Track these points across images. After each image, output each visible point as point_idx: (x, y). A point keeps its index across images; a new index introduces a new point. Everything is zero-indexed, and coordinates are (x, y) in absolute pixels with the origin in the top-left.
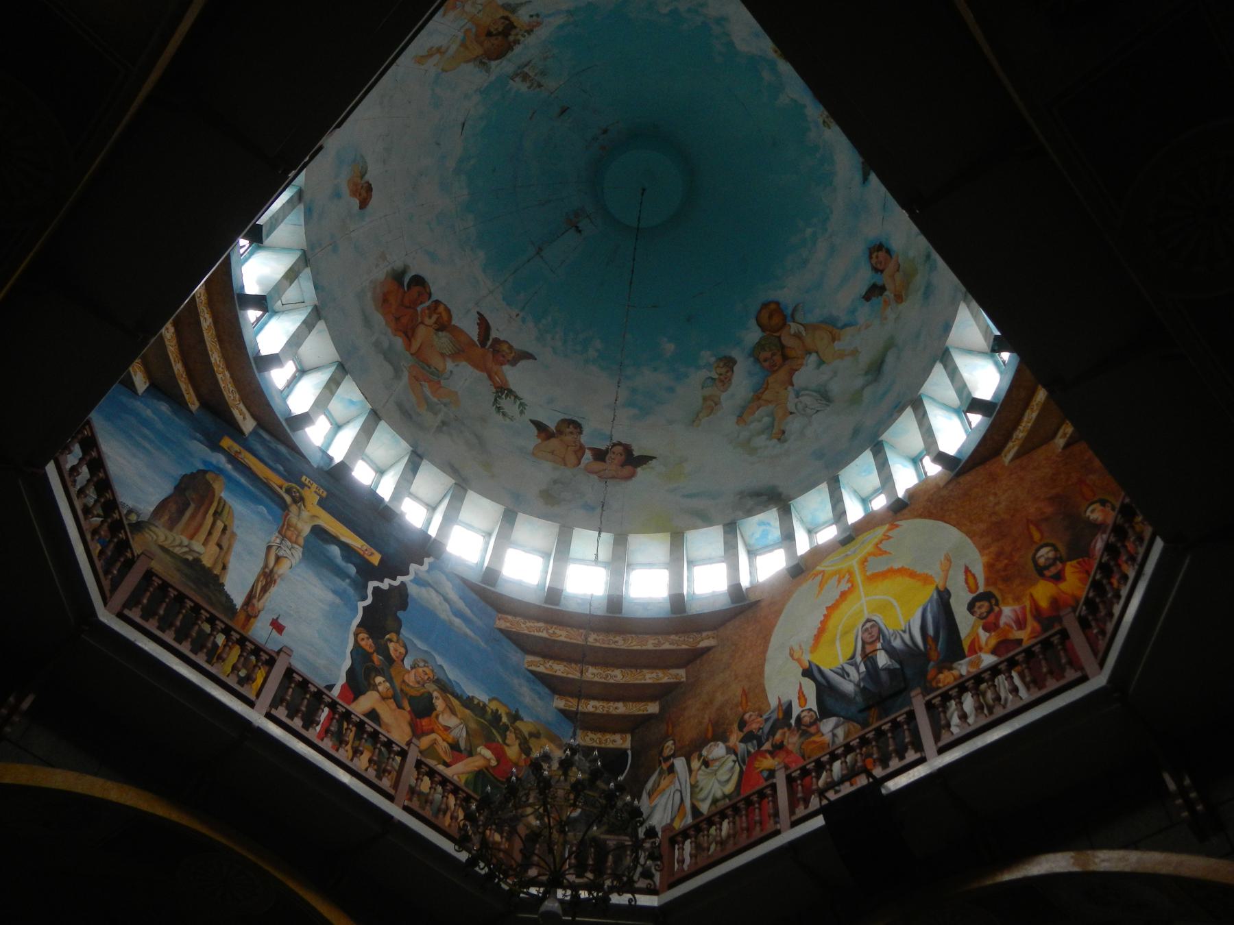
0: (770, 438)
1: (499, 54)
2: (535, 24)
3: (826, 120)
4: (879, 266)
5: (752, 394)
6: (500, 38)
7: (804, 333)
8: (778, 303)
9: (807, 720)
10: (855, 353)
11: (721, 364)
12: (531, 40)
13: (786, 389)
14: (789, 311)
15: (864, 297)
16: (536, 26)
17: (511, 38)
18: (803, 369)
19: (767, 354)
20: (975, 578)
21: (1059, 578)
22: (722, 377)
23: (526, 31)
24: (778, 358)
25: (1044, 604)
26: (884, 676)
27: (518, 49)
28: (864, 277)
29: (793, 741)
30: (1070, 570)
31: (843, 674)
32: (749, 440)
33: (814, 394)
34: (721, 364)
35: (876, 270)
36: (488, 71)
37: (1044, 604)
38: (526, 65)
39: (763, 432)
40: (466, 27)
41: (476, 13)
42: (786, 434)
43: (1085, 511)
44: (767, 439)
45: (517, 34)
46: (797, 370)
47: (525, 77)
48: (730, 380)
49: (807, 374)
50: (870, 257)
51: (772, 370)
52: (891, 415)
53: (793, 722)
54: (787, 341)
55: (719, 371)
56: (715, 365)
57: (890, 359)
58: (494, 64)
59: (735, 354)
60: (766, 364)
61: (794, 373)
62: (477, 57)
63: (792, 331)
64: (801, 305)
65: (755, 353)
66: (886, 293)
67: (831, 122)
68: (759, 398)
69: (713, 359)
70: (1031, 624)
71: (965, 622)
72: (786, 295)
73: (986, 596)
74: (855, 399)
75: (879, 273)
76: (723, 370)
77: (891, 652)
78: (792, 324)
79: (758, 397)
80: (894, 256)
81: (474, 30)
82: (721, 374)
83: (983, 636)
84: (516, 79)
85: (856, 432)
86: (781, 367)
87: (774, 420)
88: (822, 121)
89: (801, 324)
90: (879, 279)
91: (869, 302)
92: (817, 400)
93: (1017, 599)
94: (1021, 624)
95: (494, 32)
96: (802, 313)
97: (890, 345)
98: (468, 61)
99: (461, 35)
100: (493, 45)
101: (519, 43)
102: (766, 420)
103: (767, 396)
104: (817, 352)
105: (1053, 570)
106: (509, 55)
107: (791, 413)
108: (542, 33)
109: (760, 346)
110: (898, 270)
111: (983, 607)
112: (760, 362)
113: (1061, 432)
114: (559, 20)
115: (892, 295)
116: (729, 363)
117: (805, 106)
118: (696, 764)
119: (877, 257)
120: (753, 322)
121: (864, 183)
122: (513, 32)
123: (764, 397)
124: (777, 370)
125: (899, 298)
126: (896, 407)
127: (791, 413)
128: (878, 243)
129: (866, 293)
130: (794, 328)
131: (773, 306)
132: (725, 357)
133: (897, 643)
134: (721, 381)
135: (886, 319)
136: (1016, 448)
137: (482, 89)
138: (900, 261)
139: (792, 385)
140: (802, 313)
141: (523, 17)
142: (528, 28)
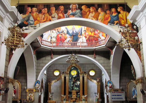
9: (65, 33)
21: (92, 33)
25: (90, 35)
26: (74, 33)
29: (63, 35)
30: (93, 32)
31: (70, 31)
37: (90, 35)
53: (64, 33)
70: (88, 36)
71: (83, 33)
73: (85, 31)
77: (75, 31)
83: (84, 34)
93: (88, 33)
94: (87, 35)
105: (92, 32)
111: (85, 32)
118: (51, 31)
133: (76, 31)
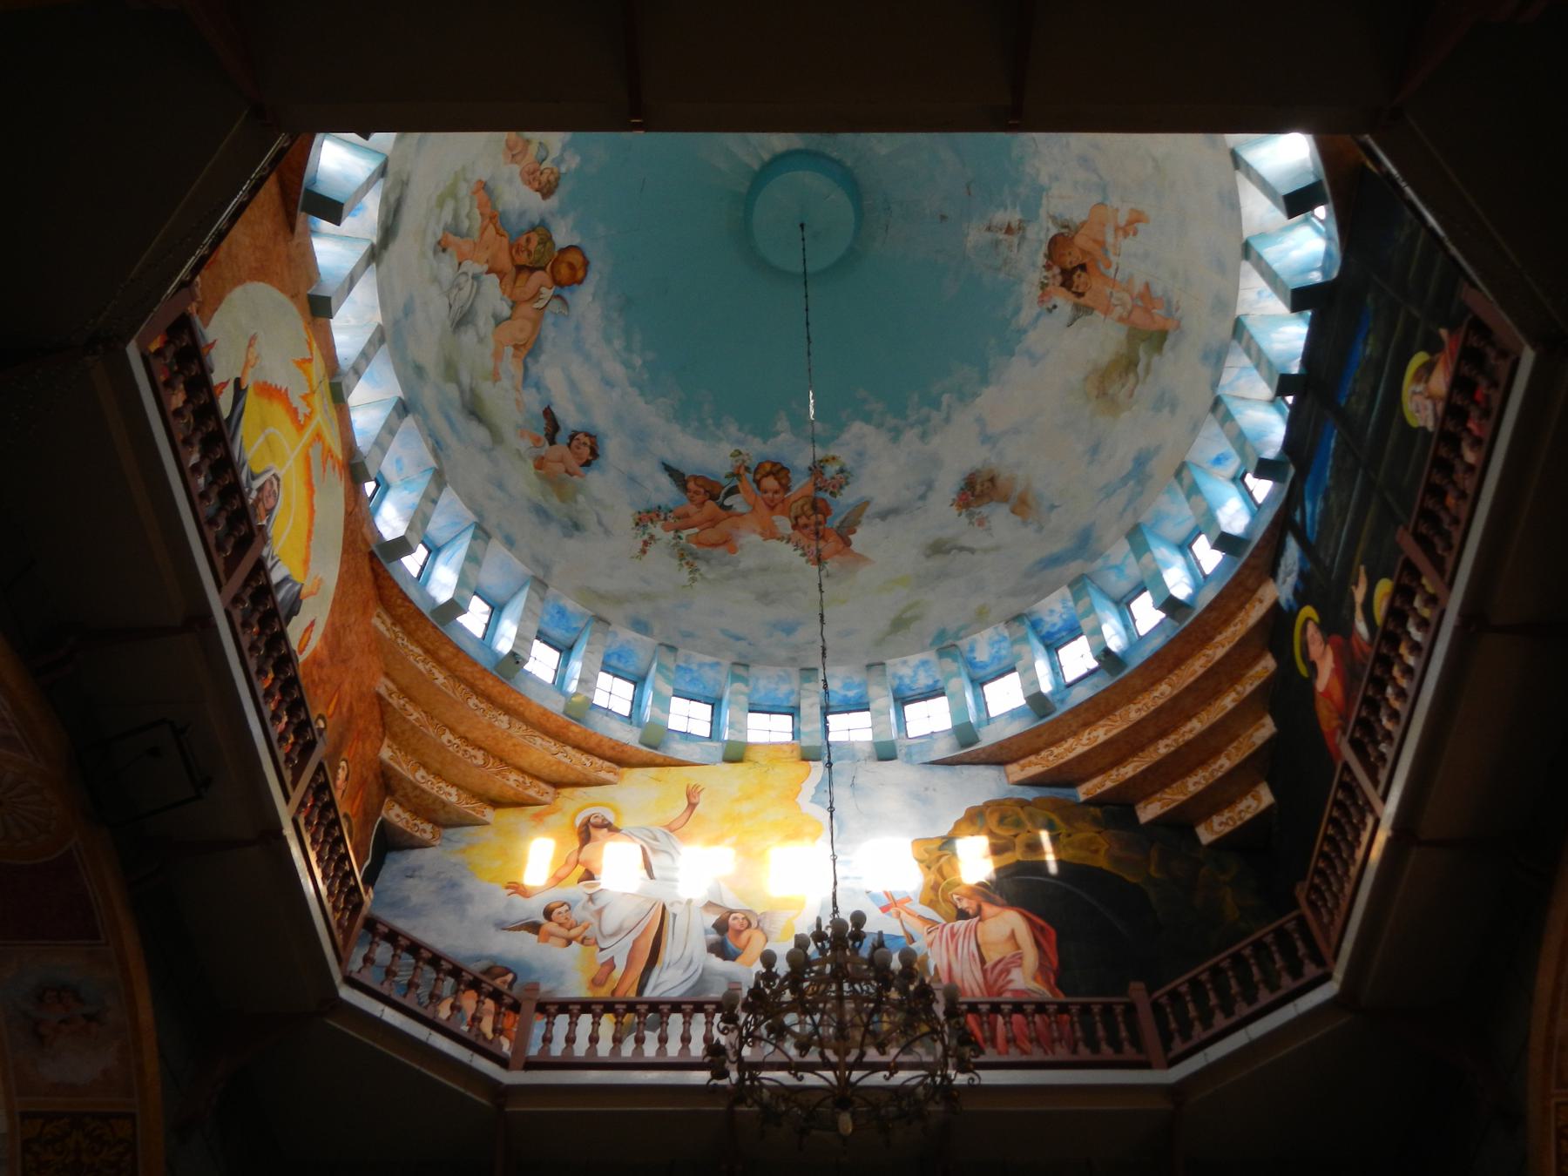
0: (446, 229)
1: (1057, 246)
2: (1045, 298)
3: (741, 457)
4: (575, 443)
5: (500, 208)
6: (1069, 267)
7: (537, 305)
8: (580, 282)
10: (495, 376)
11: (552, 178)
12: (1036, 276)
13: (487, 262)
14: (566, 293)
15: (549, 407)
16: (1042, 296)
17: (1056, 270)
18: (498, 292)
19: (533, 246)
20: (309, 638)
22: (538, 173)
23: (1047, 285)
24: (523, 259)
27: (1041, 260)
28: (570, 419)
32: (455, 197)
33: (468, 306)
34: (552, 178)
35: (572, 437)
36: (1054, 218)
38: (1019, 244)
39: (456, 216)
40: (1112, 271)
41: (1115, 295)
42: (441, 254)
43: (344, 760)
44: (446, 224)
45: (1054, 276)
46: (501, 282)
47: (1009, 230)
48: (530, 183)
49: (493, 296)
50: (587, 435)
51: (514, 248)
52: (430, 436)
54: (539, 277)
55: (548, 171)
56: (555, 170)
57: (480, 434)
58: (1054, 231)
59: (553, 202)
60: (523, 241)
61: (498, 276)
62: (1077, 232)
63: (543, 290)
64: (566, 313)
65: (542, 230)
66: (547, 443)
67: (737, 461)
68: (492, 218)
69: (563, 169)
72: (584, 298)
74: (450, 370)
75: (568, 441)
76: (544, 178)
78: (552, 290)
79: (494, 217)
80: (582, 470)
81: (1102, 268)
82: (541, 174)
84: (1017, 223)
85: (419, 370)
86: (513, 259)
87: (462, 237)
88: (742, 451)
89: (547, 304)
90: (562, 437)
91: (542, 412)
92: (462, 307)
95: (1079, 272)
96: (557, 312)
97: (496, 436)
98: (1083, 224)
99: (1113, 258)
100: (1070, 254)
101: (1044, 266)
102: (466, 224)
103: (491, 230)
104: (509, 318)
106: (1044, 249)
107: (460, 264)
108: (1029, 289)
109: (547, 239)
110: (567, 471)
112: (529, 232)
113: (391, 686)
114: (1025, 316)
115: (543, 454)
116: (546, 191)
117: (765, 443)
119: (585, 444)
120: (576, 241)
121: (664, 464)
122: (1059, 279)
123: (491, 226)
124: (511, 254)
125: (540, 463)
126: (437, 443)
127: (460, 264)
128: (599, 452)
129: (552, 413)
130: (547, 293)
131: (580, 274)
132: (557, 186)
134: (533, 173)
135: (522, 436)
136: (387, 634)
137: (1045, 193)
138: (575, 477)
139: (489, 272)
140: (557, 312)
141: (1064, 302)
142: (1048, 289)
